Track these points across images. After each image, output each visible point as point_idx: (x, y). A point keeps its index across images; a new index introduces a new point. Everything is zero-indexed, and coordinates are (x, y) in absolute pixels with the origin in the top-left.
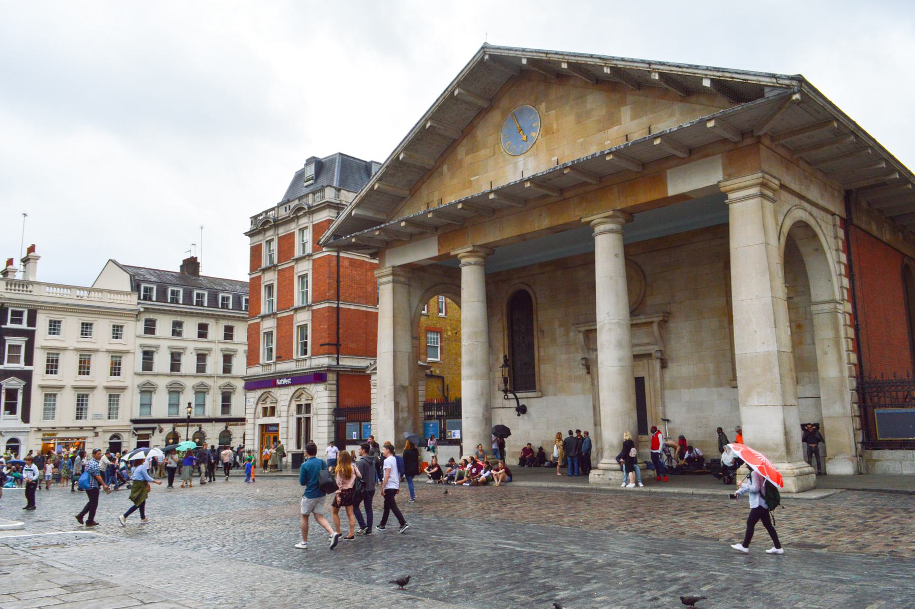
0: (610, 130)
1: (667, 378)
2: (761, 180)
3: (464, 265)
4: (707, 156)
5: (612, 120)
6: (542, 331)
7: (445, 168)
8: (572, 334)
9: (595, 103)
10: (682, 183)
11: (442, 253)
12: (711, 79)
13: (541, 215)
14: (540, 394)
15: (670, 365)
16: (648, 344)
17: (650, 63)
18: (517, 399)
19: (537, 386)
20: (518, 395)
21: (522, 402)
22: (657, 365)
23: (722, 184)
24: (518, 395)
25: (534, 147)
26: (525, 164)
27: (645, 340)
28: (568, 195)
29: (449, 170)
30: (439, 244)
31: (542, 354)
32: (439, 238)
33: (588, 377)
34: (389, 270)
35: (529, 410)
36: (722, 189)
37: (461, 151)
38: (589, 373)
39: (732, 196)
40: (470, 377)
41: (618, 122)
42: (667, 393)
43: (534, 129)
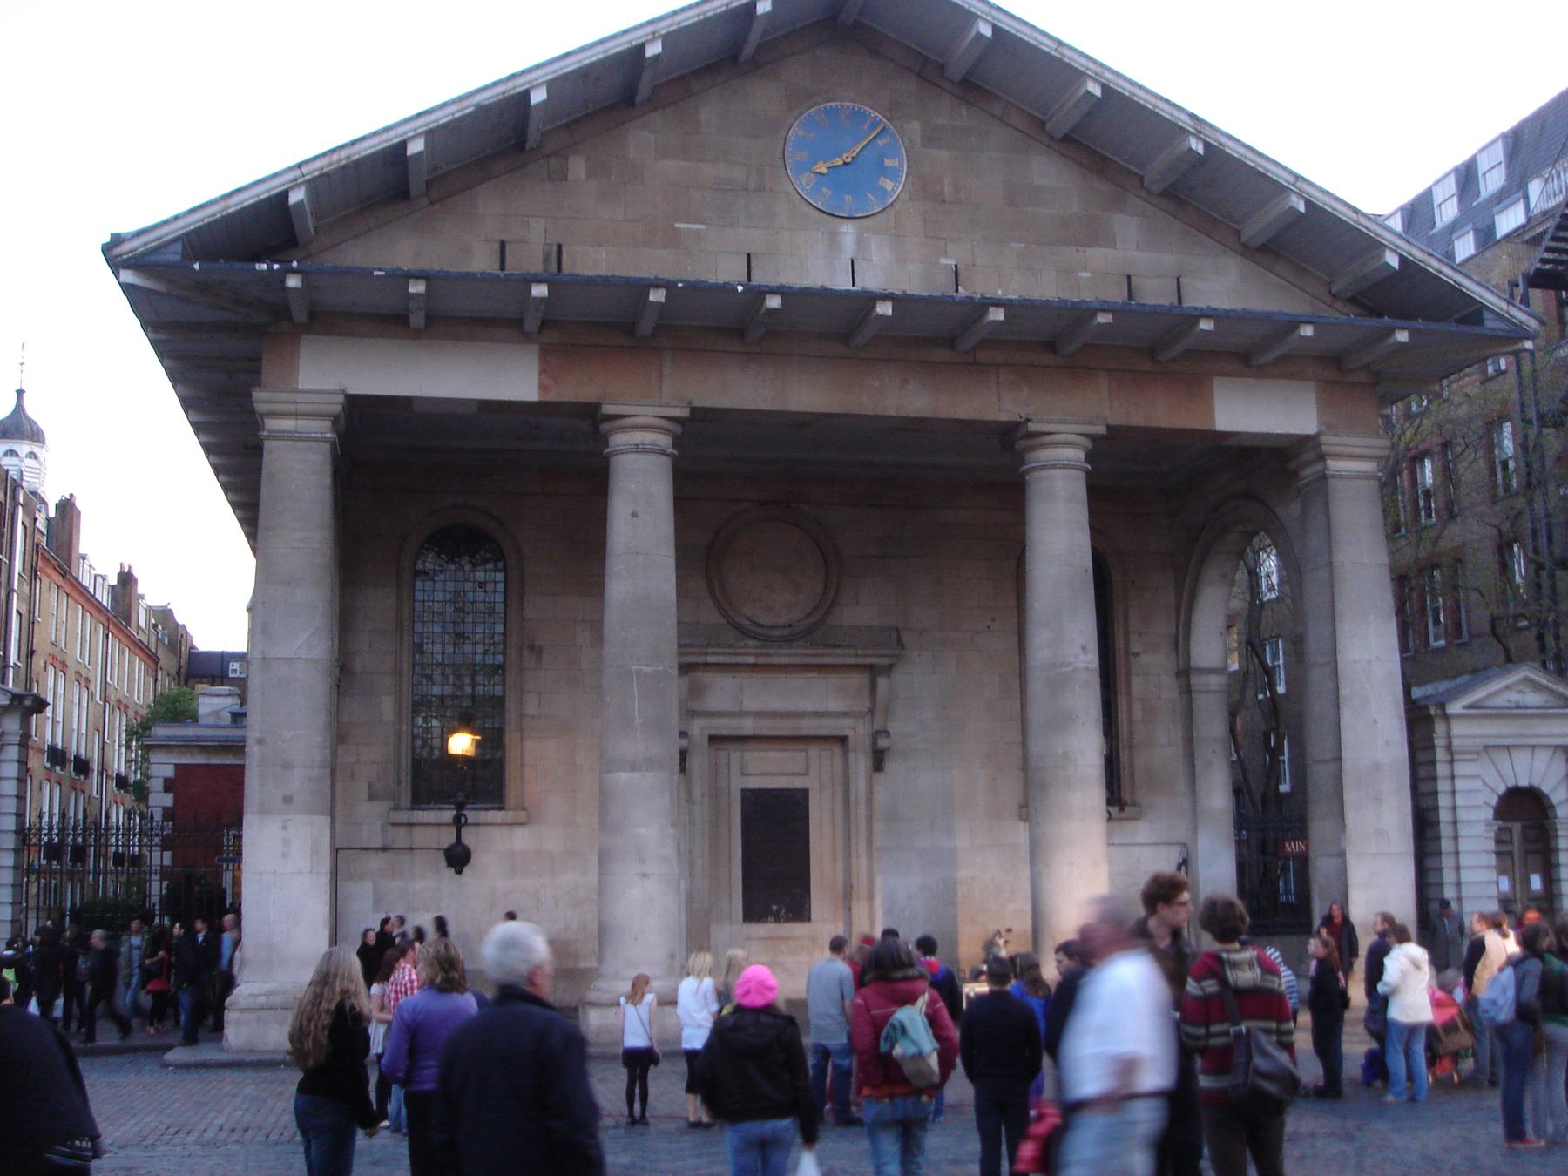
0: (1090, 251)
1: (881, 799)
2: (1385, 453)
3: (638, 449)
4: (1291, 376)
5: (1094, 234)
7: (577, 167)
9: (1049, 174)
10: (1247, 411)
11: (552, 397)
12: (1401, 256)
13: (905, 381)
14: (522, 816)
15: (889, 765)
16: (845, 714)
17: (1298, 177)
21: (468, 838)
22: (861, 763)
23: (1323, 439)
24: (471, 815)
25: (891, 213)
26: (860, 243)
27: (834, 705)
28: (983, 356)
29: (590, 174)
30: (542, 371)
32: (546, 353)
34: (336, 405)
36: (1325, 448)
37: (642, 140)
38: (683, 768)
39: (1334, 465)
41: (1110, 242)
42: (878, 827)
43: (893, 174)
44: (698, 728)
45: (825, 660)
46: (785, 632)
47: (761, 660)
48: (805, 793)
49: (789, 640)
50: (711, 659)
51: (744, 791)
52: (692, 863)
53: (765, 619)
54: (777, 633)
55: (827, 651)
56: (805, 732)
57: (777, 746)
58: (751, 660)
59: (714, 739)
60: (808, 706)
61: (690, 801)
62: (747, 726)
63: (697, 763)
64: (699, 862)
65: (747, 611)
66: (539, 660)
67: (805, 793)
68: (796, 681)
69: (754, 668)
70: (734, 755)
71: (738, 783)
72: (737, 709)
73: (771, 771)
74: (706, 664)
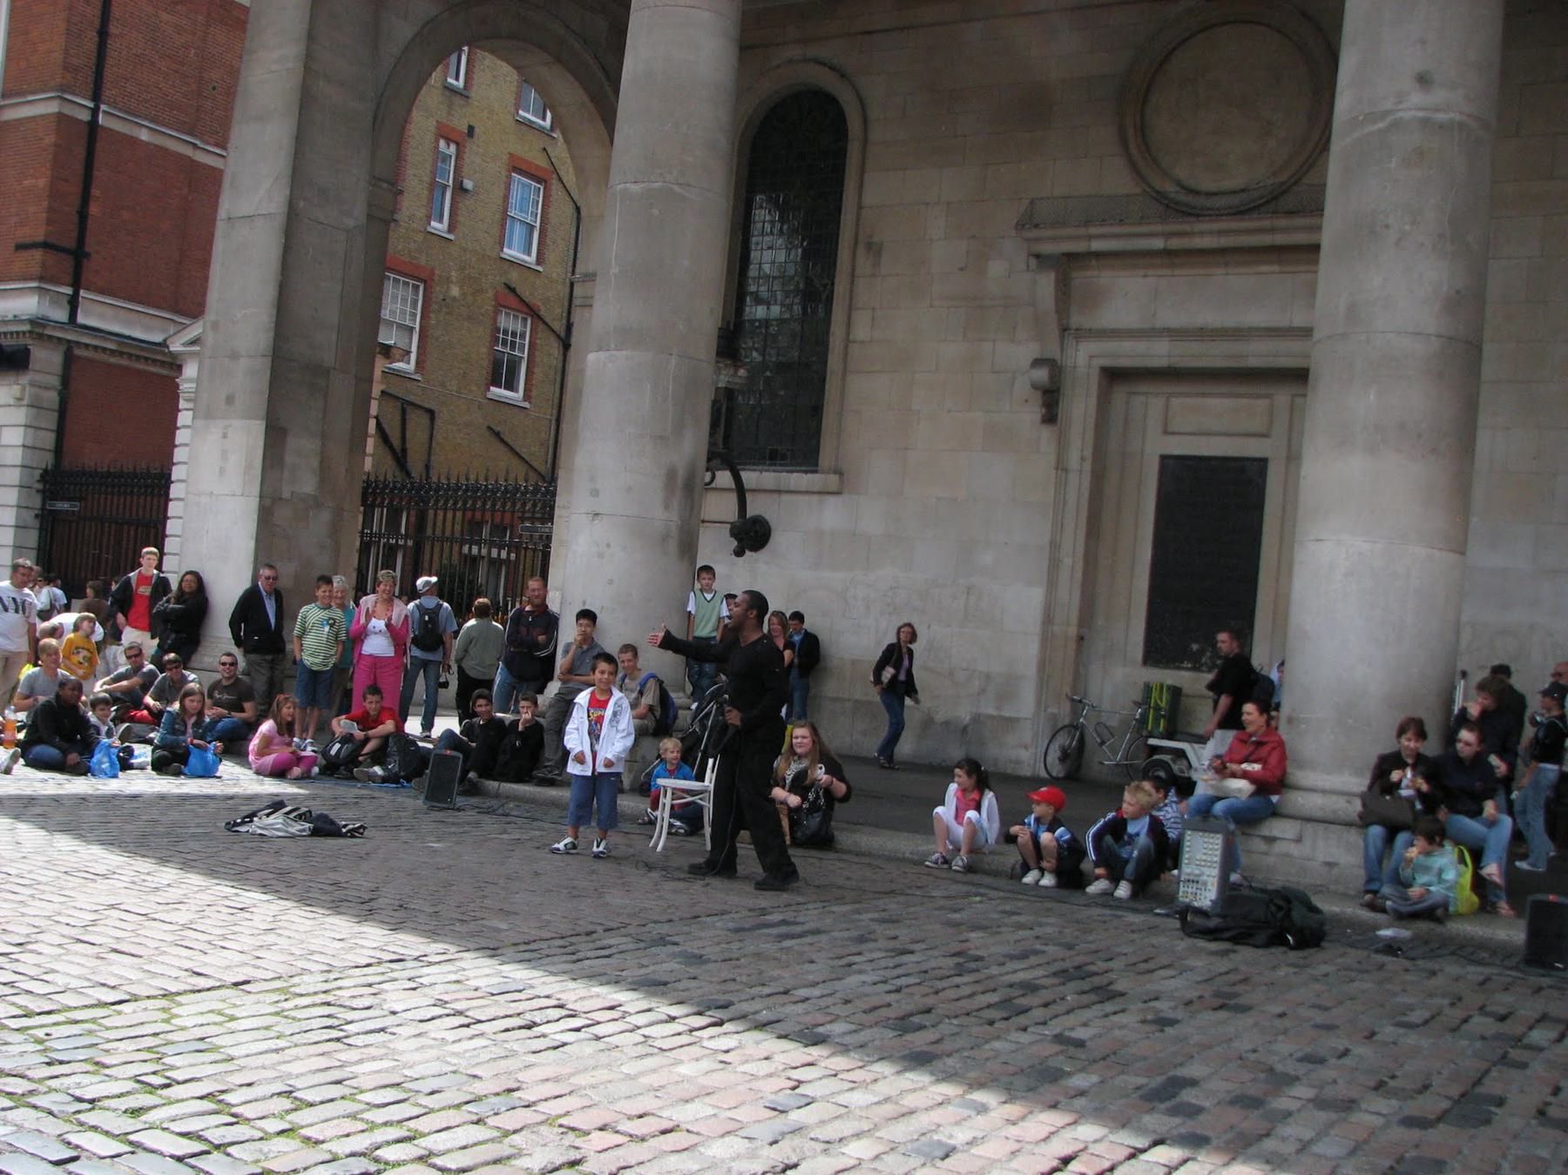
6: (874, 249)
8: (996, 268)
14: (833, 480)
18: (741, 491)
19: (826, 457)
20: (750, 477)
24: (750, 477)
31: (861, 331)
33: (1046, 433)
35: (778, 539)
38: (1050, 418)
40: (627, 337)
44: (1085, 358)
45: (1280, 239)
46: (1235, 200)
47: (1175, 243)
48: (1262, 463)
49: (1240, 212)
50: (1096, 245)
51: (1163, 458)
52: (1054, 564)
53: (1207, 184)
54: (1220, 202)
55: (1282, 222)
56: (1253, 362)
57: (1224, 389)
58: (1158, 244)
59: (1114, 376)
60: (1256, 317)
61: (1061, 466)
62: (1159, 353)
63: (1080, 406)
64: (1068, 561)
65: (1181, 172)
66: (877, 265)
67: (1263, 462)
68: (1240, 279)
69: (1171, 257)
70: (1150, 404)
71: (1155, 446)
72: (1146, 326)
73: (1210, 427)
74: (1098, 255)
